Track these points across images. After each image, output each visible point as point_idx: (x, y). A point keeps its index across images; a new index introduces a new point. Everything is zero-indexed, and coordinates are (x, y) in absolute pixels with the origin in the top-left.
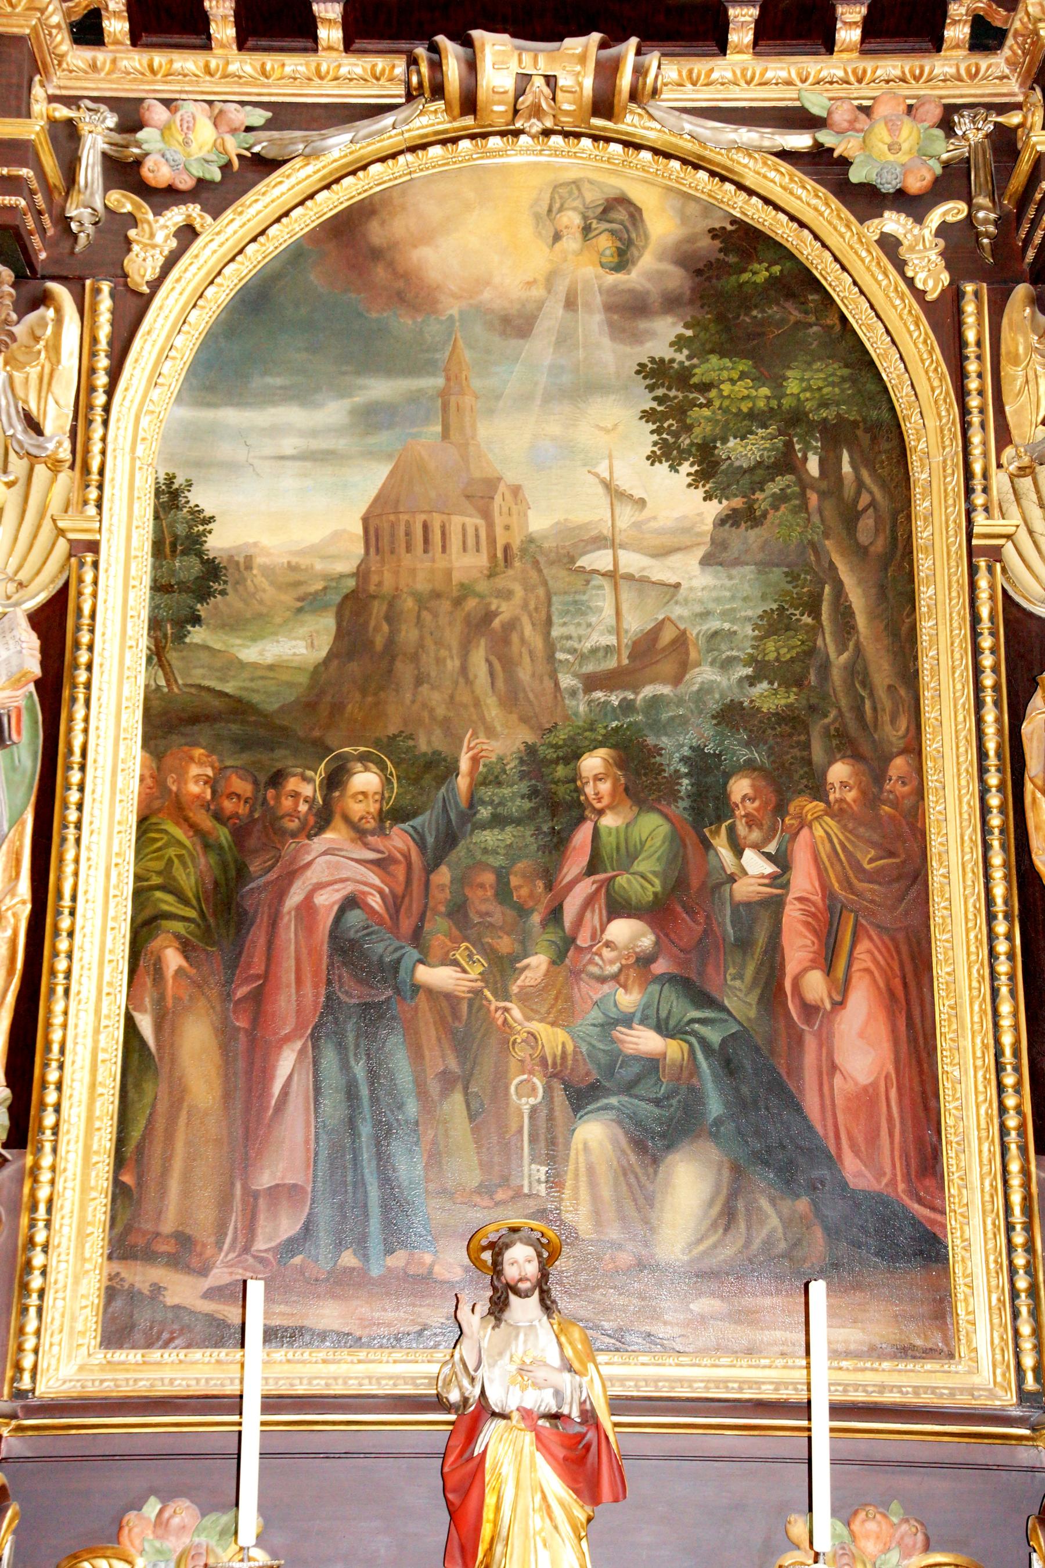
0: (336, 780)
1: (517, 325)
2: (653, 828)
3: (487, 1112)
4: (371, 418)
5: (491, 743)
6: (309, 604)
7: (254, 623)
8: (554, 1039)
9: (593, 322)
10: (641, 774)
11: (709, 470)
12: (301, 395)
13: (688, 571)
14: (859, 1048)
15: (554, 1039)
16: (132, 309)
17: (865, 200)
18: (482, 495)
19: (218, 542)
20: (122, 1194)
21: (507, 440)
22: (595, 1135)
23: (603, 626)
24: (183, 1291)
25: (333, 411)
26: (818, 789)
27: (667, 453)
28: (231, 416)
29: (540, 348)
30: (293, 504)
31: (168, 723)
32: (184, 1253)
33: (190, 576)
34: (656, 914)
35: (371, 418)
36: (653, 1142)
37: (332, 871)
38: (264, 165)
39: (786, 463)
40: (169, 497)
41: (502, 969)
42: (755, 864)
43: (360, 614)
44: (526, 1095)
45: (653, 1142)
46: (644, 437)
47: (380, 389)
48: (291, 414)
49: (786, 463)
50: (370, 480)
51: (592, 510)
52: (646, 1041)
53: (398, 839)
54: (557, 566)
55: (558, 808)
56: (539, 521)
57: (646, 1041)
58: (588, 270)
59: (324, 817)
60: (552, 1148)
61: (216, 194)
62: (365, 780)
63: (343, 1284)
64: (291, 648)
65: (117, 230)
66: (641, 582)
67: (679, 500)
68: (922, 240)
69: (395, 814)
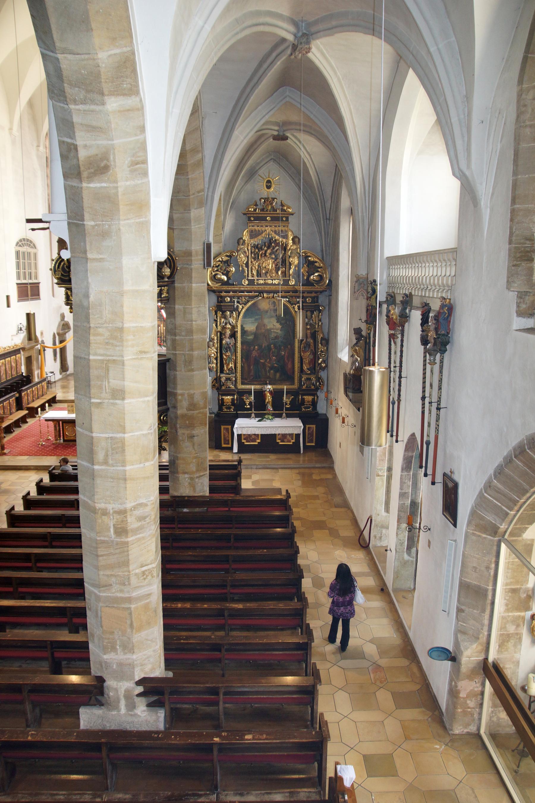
0: (254, 347)
1: (267, 312)
2: (276, 350)
3: (265, 370)
4: (256, 320)
5: (265, 344)
6: (252, 334)
7: (248, 336)
8: (269, 365)
9: (272, 312)
10: (275, 347)
11: (281, 324)
12: (251, 318)
13: (279, 331)
14: (290, 366)
15: (269, 365)
16: (239, 313)
17: (292, 304)
18: (264, 325)
19: (245, 329)
20: (241, 376)
21: (266, 321)
22: (272, 371)
23: (273, 335)
24: (246, 381)
25: (253, 319)
26: (288, 347)
27: (277, 322)
28: (246, 319)
29: (268, 314)
30: (251, 327)
31: (242, 343)
32: (246, 379)
33: (244, 332)
34: (275, 356)
35: (256, 320)
36: (276, 372)
37: (254, 354)
38: (248, 301)
39: (286, 323)
40: (242, 326)
41: (266, 361)
42: (283, 353)
43: (256, 335)
44: (268, 369)
45: (276, 372)
46: (276, 321)
47: (257, 317)
48: (250, 319)
49: (286, 323)
50: (256, 324)
51: (272, 327)
52: (276, 365)
53: (259, 351)
54: (269, 331)
55: (270, 349)
56: (268, 328)
57: (276, 365)
58: (272, 308)
59: (254, 349)
60: (269, 372)
61: (245, 304)
62: (256, 347)
63: (256, 381)
64: (251, 337)
65: (238, 306)
66: (276, 332)
67: (278, 326)
68: (296, 307)
69: (258, 350)
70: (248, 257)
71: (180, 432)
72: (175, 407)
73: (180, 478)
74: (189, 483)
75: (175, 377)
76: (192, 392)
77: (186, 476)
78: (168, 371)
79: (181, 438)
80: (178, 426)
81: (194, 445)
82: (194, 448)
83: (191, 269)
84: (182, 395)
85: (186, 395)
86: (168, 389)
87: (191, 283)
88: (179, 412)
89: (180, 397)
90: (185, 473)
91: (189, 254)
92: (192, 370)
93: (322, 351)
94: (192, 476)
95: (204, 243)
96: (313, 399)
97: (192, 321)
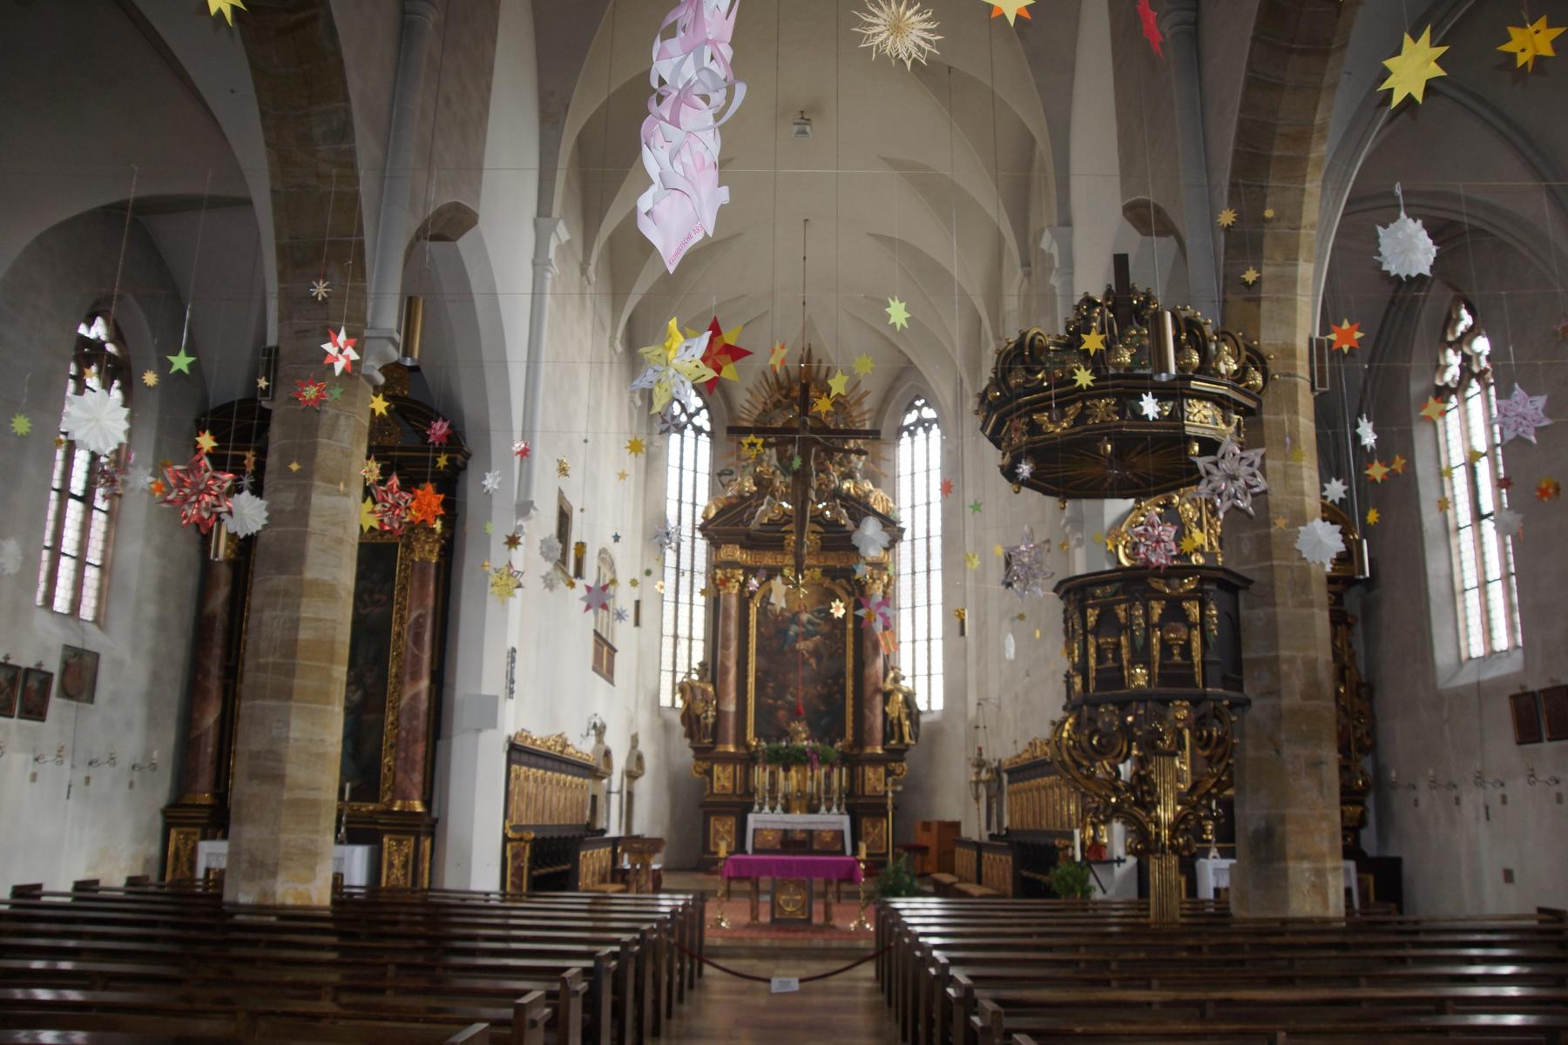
70: (1200, 510)
71: (1288, 751)
72: (1272, 692)
73: (1291, 872)
74: (1314, 886)
75: (1272, 621)
76: (1312, 654)
77: (1306, 865)
78: (1243, 613)
79: (1289, 767)
80: (1283, 737)
81: (1321, 784)
82: (1321, 791)
83: (1296, 385)
84: (1291, 661)
85: (1299, 662)
86: (1244, 656)
87: (1296, 412)
88: (1286, 702)
89: (1285, 667)
90: (1302, 857)
91: (1289, 352)
92: (1311, 604)
93: (1361, 712)
94: (1319, 865)
95: (1311, 340)
96: (1363, 814)
97: (1302, 493)
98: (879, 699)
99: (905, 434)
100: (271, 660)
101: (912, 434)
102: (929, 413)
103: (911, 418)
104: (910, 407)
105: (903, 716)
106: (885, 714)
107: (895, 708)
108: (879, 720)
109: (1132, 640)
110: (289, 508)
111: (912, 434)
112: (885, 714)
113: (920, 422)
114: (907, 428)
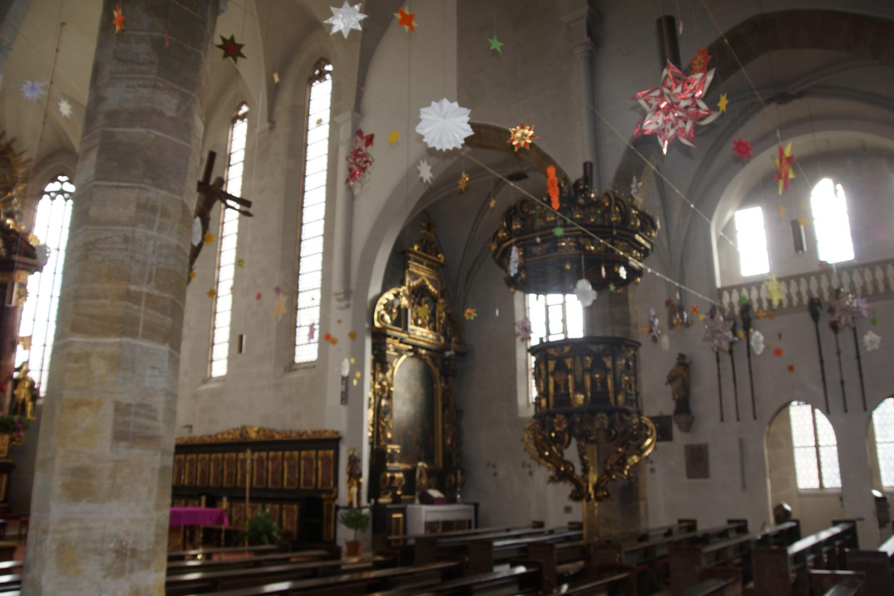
98: (9, 385)
99: (46, 197)
100: (145, 289)
101: (53, 199)
102: (70, 188)
103: (51, 187)
104: (54, 179)
105: (28, 398)
106: (13, 396)
107: (22, 393)
108: (8, 400)
109: (575, 377)
110: (169, 114)
111: (53, 199)
112: (13, 396)
113: (62, 192)
114: (48, 193)
